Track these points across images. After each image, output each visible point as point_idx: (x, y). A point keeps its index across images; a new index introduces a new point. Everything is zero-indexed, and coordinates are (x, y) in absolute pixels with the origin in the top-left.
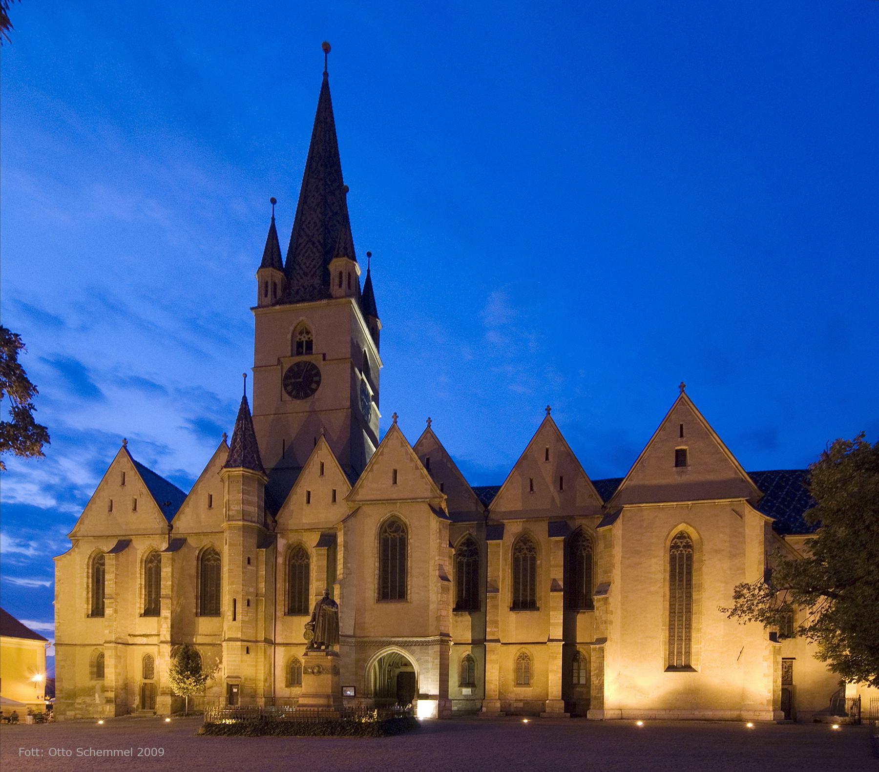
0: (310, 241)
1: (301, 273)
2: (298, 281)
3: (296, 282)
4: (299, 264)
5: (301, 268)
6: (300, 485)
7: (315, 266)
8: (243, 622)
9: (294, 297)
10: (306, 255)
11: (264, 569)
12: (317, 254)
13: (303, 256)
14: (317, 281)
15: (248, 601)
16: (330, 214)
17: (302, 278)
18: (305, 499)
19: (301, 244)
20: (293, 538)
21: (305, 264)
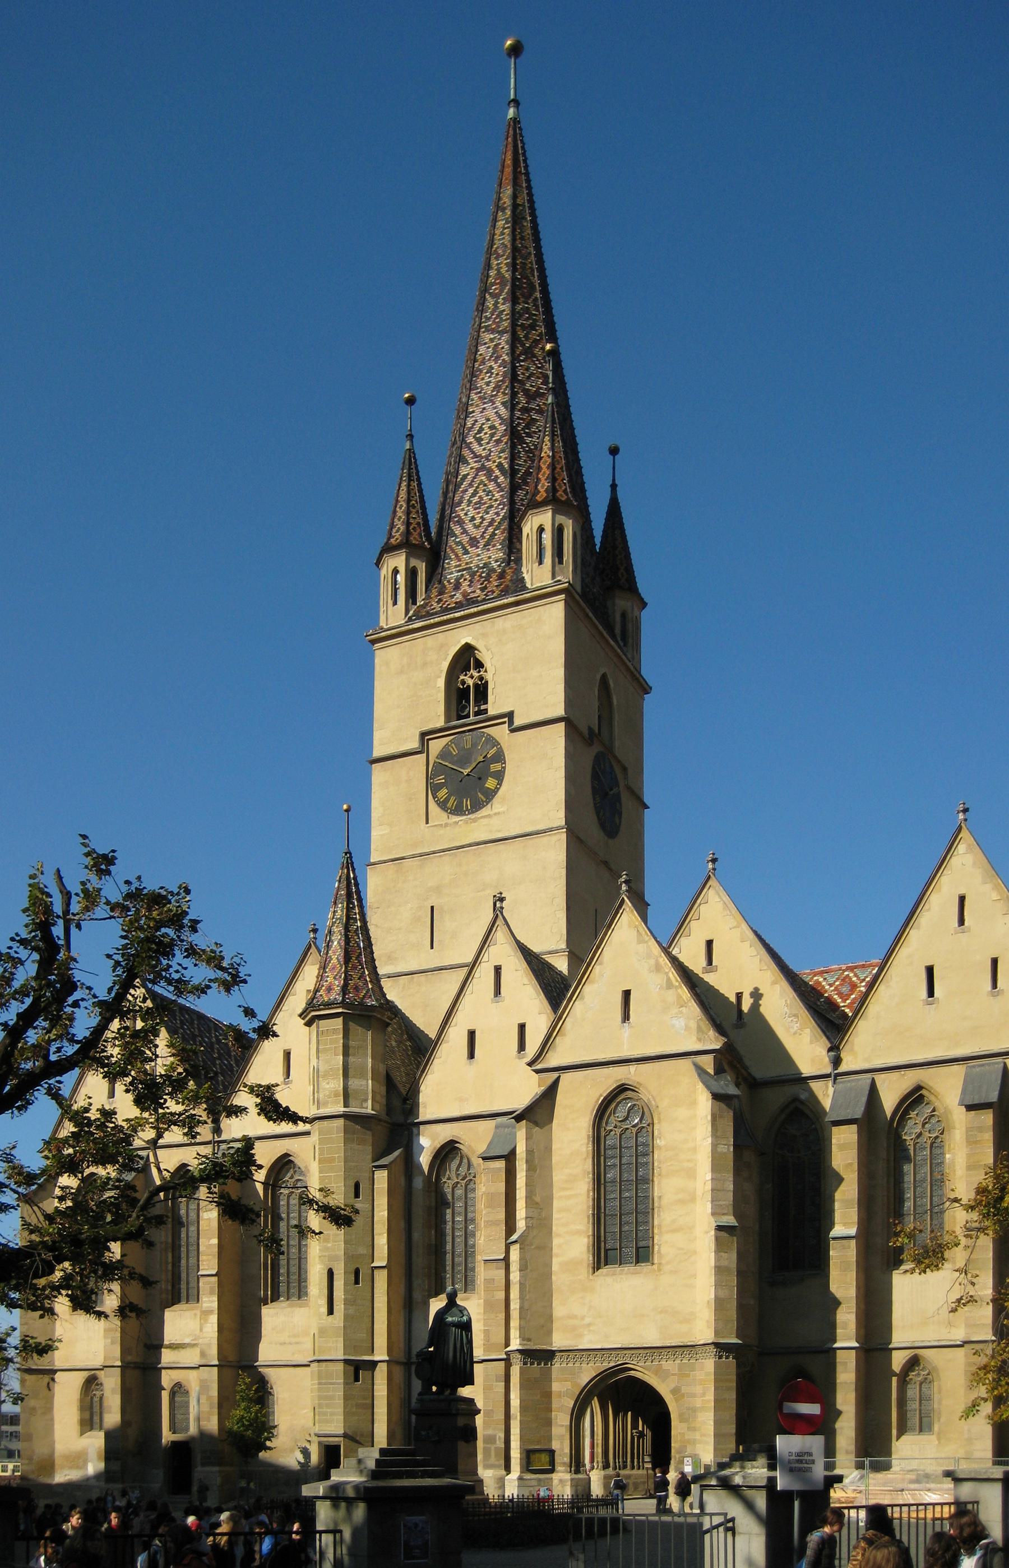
1: (465, 539)
3: (453, 563)
4: (461, 522)
5: (465, 532)
7: (491, 524)
8: (347, 1317)
9: (452, 597)
10: (476, 499)
11: (386, 1207)
12: (497, 495)
14: (495, 555)
15: (357, 1272)
16: (522, 399)
17: (466, 552)
19: (465, 477)
20: (445, 1133)
21: (473, 519)
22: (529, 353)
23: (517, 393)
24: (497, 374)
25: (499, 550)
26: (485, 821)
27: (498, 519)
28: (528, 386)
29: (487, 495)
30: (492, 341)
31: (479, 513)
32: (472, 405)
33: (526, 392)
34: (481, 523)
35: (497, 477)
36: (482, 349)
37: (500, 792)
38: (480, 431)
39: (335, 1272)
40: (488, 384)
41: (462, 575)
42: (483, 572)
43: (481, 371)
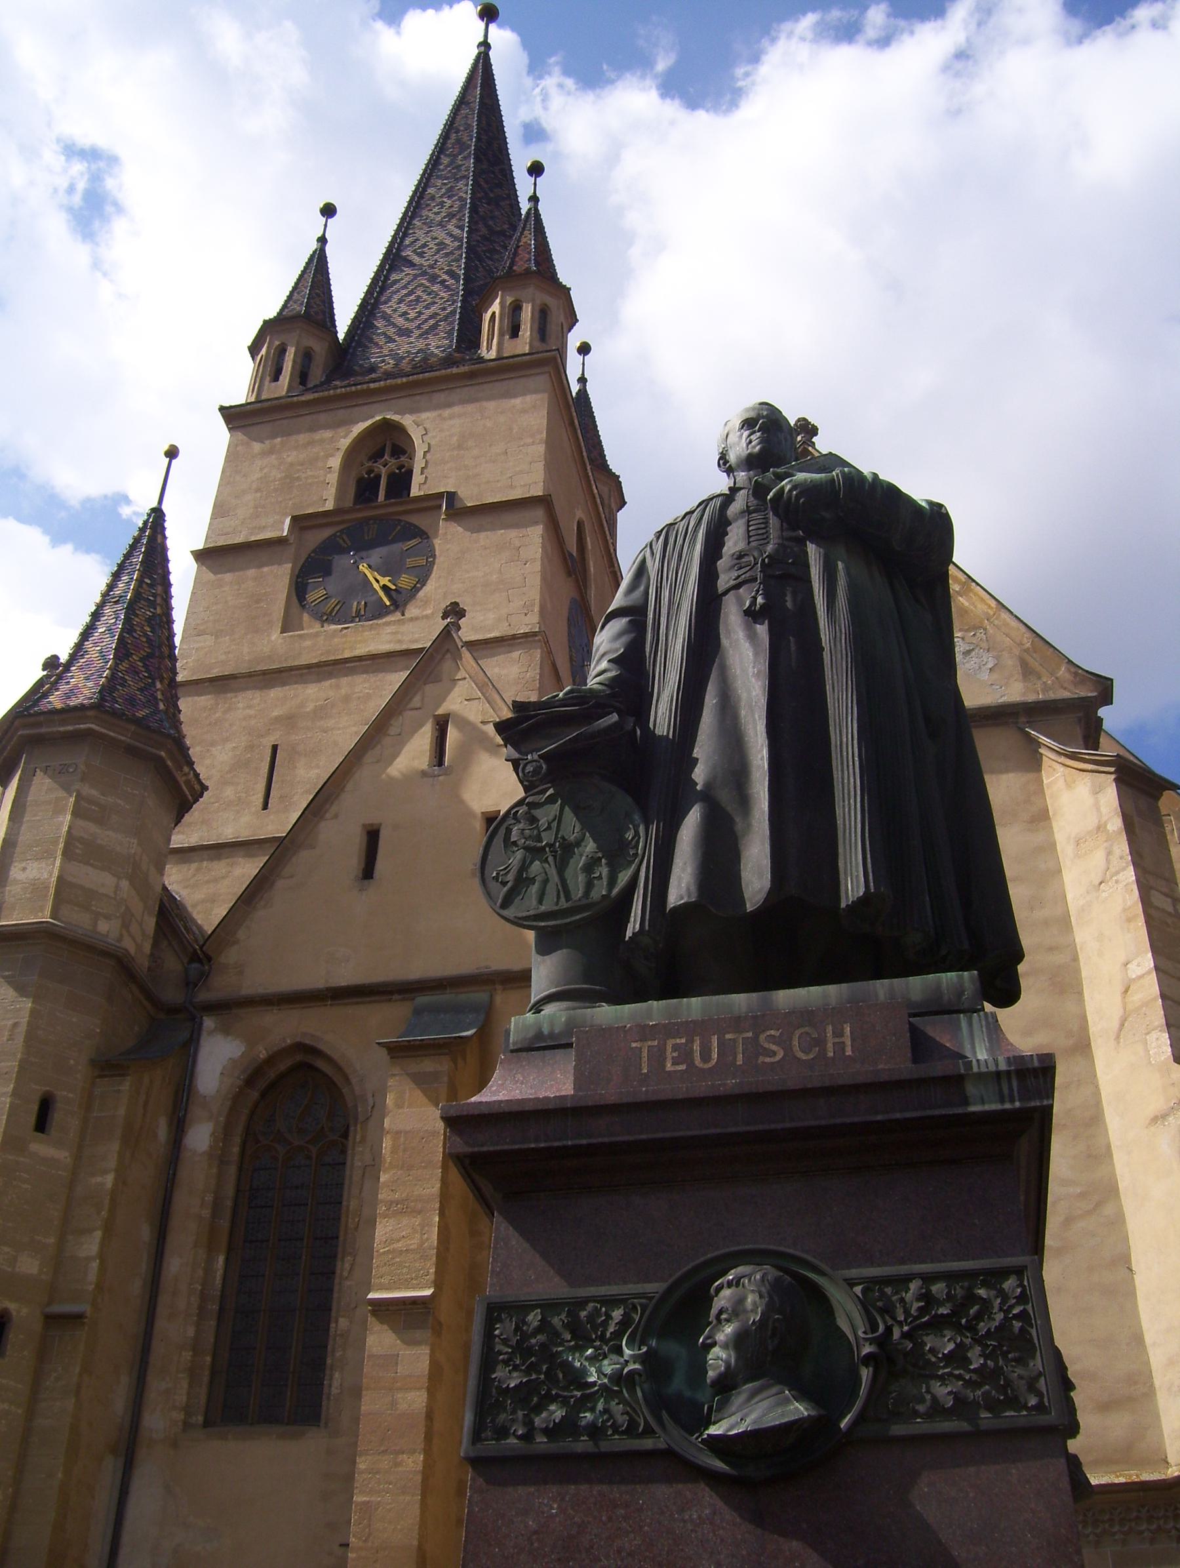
0: (424, 273)
4: (387, 318)
6: (334, 809)
7: (431, 317)
12: (443, 294)
13: (400, 301)
16: (484, 231)
18: (354, 861)
19: (395, 282)
23: (476, 223)
24: (451, 207)
25: (444, 338)
26: (389, 629)
27: (443, 314)
28: (491, 223)
29: (429, 294)
30: (445, 184)
31: (416, 309)
32: (413, 228)
35: (445, 281)
36: (431, 191)
37: (421, 594)
38: (424, 245)
40: (436, 214)
41: (383, 361)
42: (416, 357)
43: (428, 205)
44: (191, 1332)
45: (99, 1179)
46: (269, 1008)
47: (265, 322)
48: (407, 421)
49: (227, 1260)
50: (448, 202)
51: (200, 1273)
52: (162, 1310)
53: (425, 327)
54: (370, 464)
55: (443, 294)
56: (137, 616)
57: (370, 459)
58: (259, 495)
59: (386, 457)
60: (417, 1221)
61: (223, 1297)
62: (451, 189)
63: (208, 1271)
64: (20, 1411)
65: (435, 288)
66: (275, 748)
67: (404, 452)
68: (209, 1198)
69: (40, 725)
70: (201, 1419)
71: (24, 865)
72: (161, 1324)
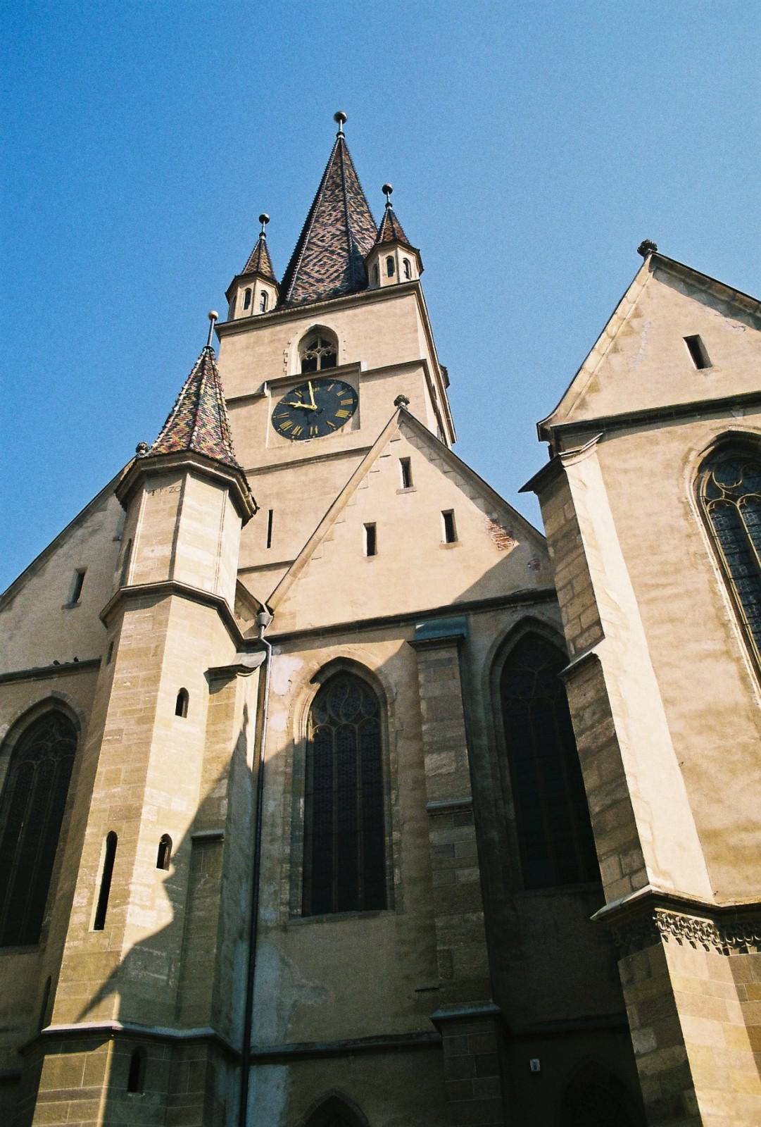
0: (327, 250)
2: (304, 288)
5: (313, 278)
13: (314, 265)
16: (358, 228)
17: (313, 285)
19: (309, 256)
22: (361, 213)
27: (341, 270)
28: (360, 224)
29: (331, 260)
33: (360, 227)
34: (325, 273)
38: (323, 236)
39: (120, 839)
44: (288, 850)
45: (222, 745)
46: (317, 637)
47: (236, 277)
48: (331, 325)
49: (305, 802)
50: (334, 214)
51: (290, 810)
52: (265, 838)
53: (333, 277)
54: (309, 352)
55: (340, 260)
56: (206, 404)
57: (308, 350)
58: (243, 372)
59: (319, 347)
60: (452, 754)
61: (305, 826)
62: (333, 208)
63: (295, 810)
64: (181, 907)
65: (334, 257)
66: (271, 512)
67: (329, 344)
68: (290, 761)
69: (154, 463)
70: (299, 910)
71: (152, 548)
72: (265, 846)
